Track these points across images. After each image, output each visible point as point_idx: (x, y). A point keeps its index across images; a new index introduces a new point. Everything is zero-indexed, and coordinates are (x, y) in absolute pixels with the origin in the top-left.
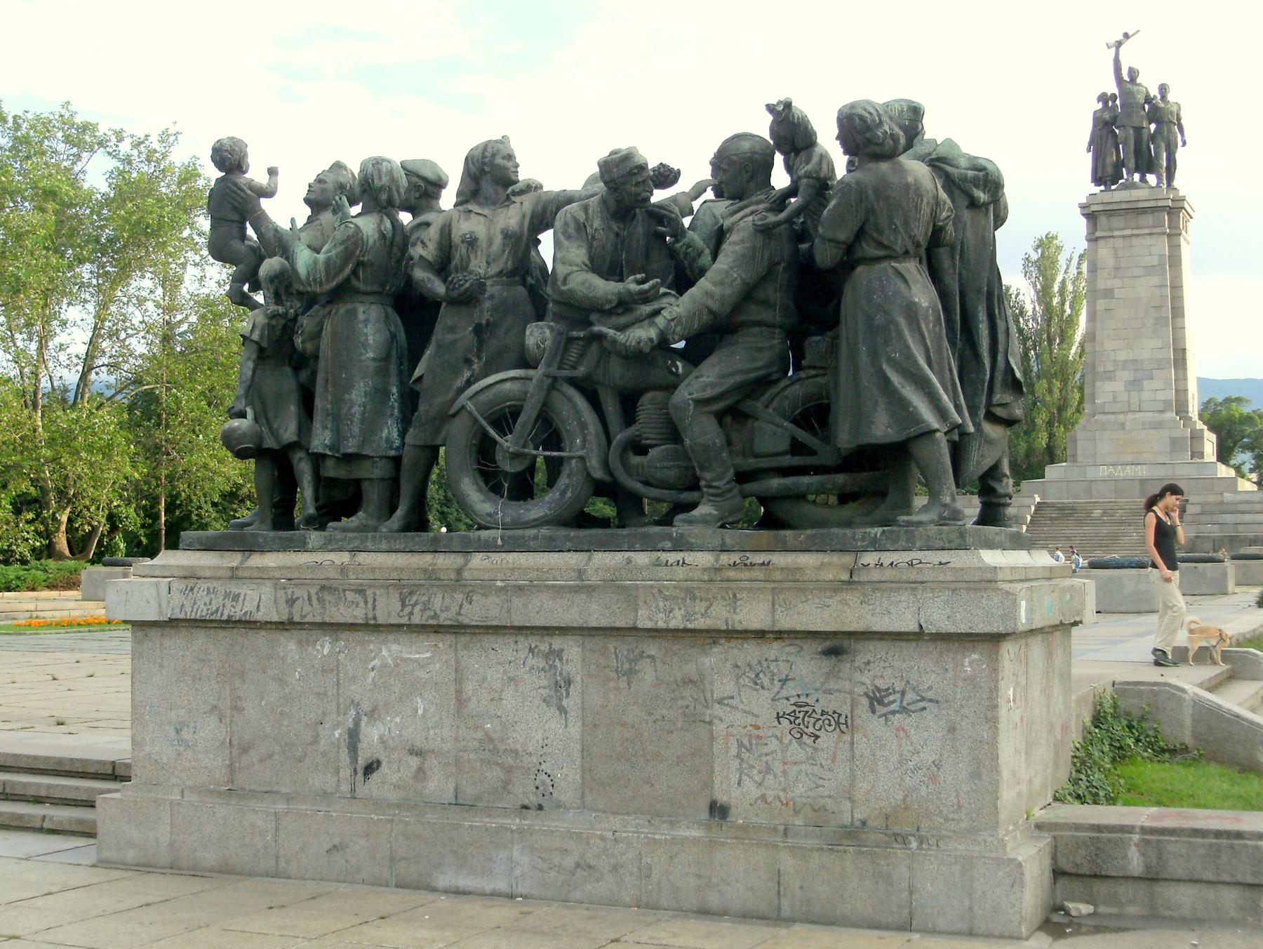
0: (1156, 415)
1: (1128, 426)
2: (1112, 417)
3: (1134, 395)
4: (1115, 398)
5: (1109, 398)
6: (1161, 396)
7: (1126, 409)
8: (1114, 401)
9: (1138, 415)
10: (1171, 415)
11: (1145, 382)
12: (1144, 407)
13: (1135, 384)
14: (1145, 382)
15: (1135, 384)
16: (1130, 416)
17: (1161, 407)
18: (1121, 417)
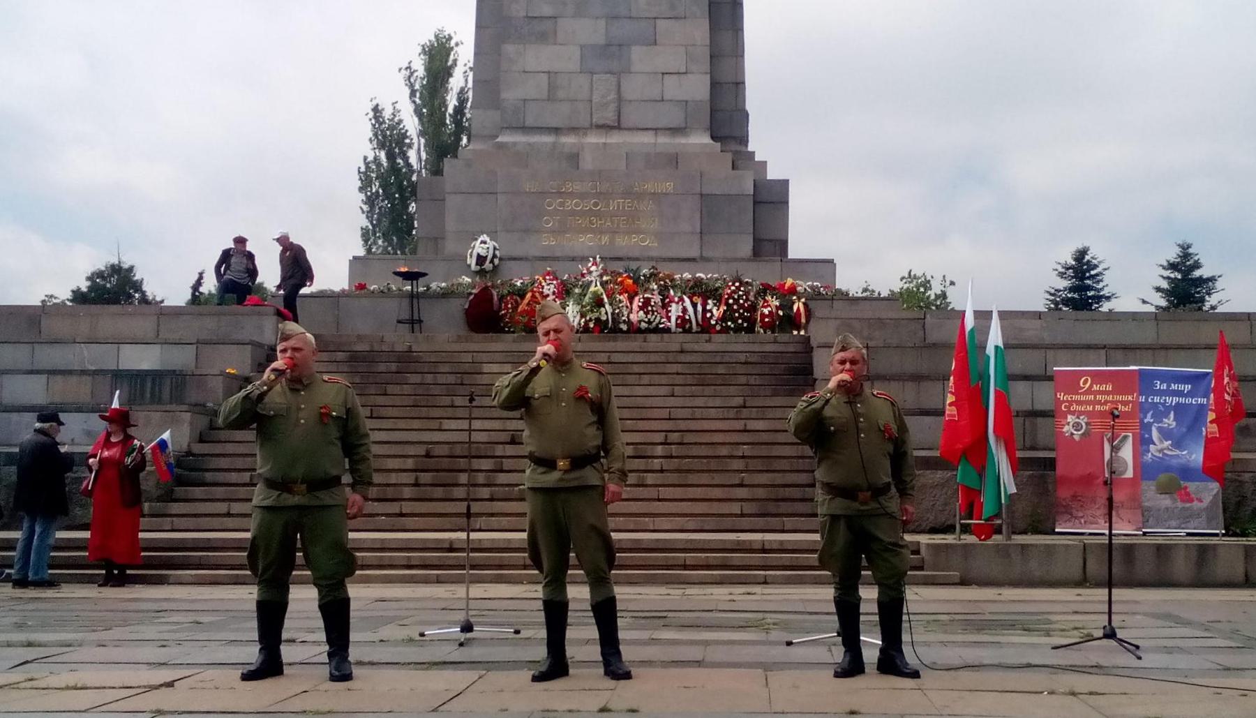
0: (663, 140)
1: (587, 162)
2: (548, 139)
3: (603, 86)
4: (552, 88)
5: (534, 88)
6: (673, 89)
7: (583, 120)
8: (551, 98)
9: (615, 138)
10: (701, 139)
11: (637, 52)
12: (632, 116)
13: (610, 55)
14: (637, 52)
15: (610, 55)
16: (593, 139)
17: (676, 118)
18: (568, 140)
